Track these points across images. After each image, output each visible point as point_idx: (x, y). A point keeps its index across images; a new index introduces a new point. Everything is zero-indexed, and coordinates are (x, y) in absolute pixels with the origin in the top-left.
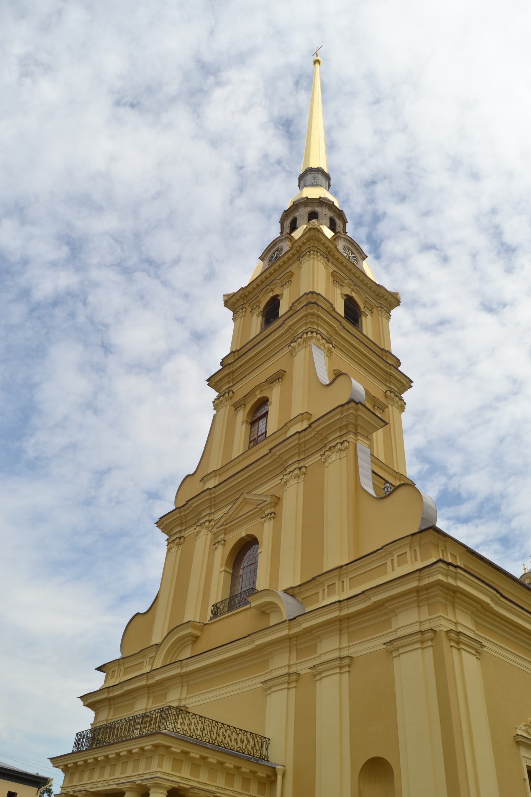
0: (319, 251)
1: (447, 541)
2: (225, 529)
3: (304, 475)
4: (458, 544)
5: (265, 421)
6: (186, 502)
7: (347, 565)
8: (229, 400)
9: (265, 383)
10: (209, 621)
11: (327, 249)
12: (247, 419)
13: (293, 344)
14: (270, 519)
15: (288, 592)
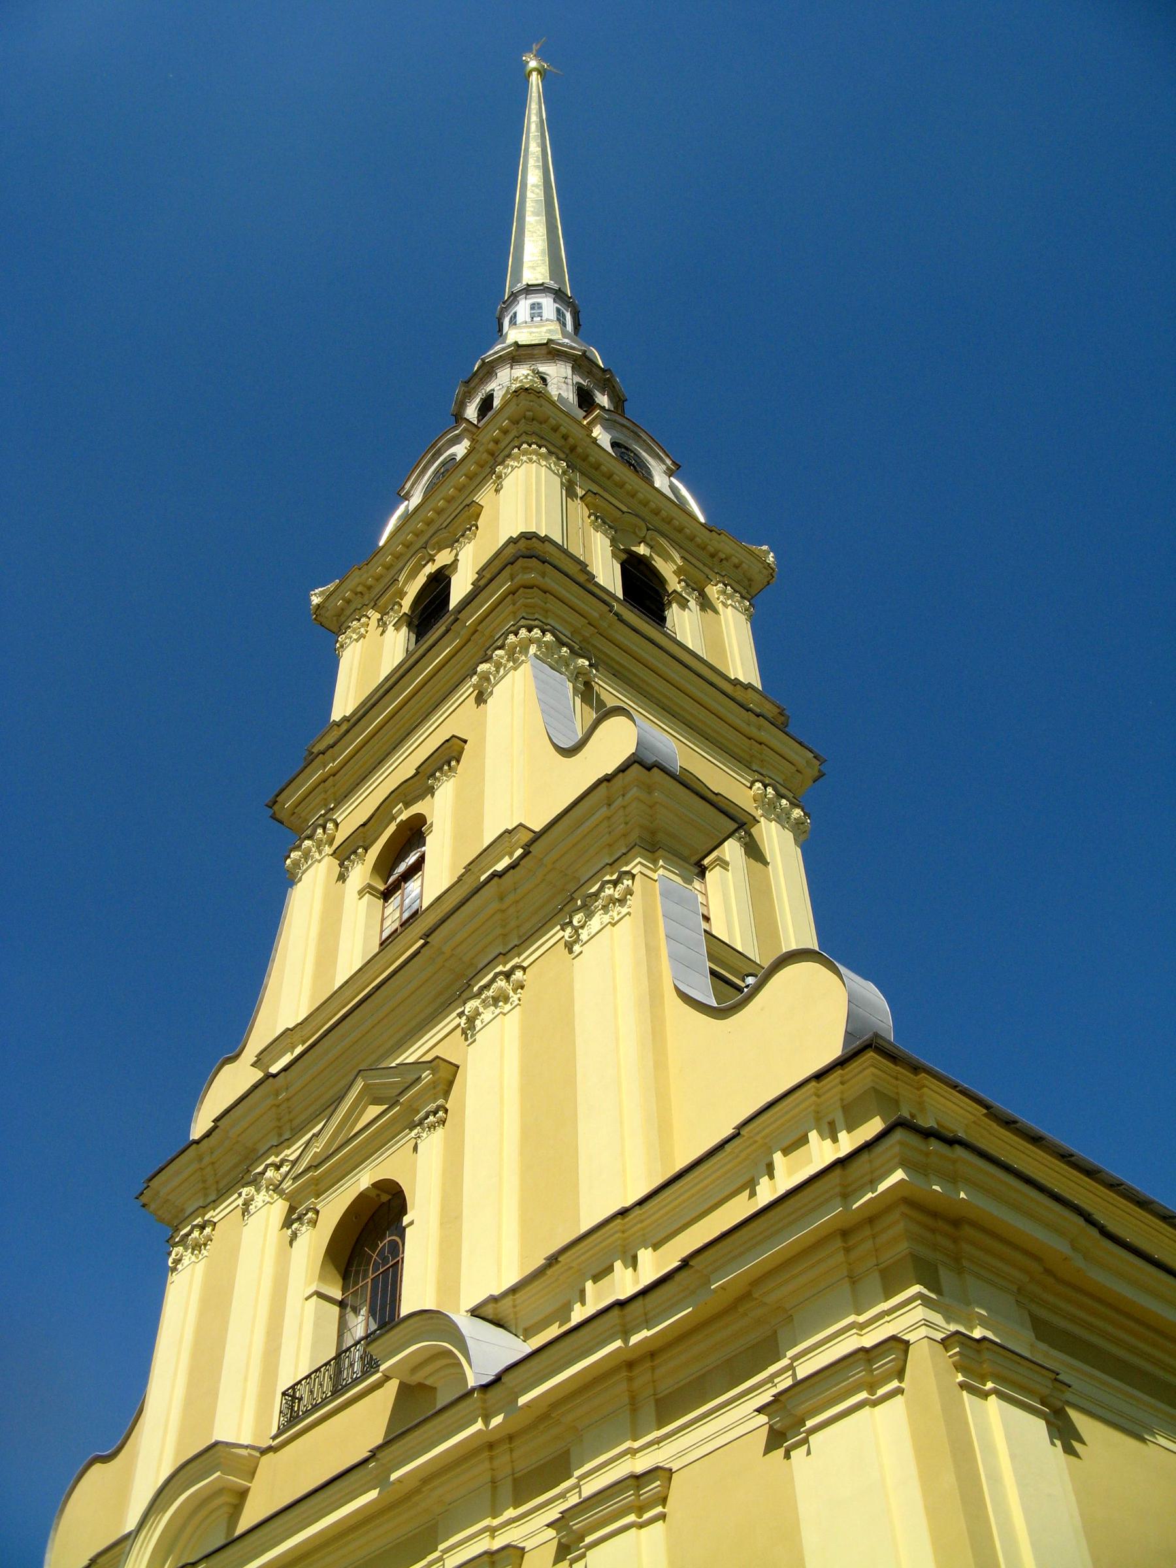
0: (543, 442)
1: (924, 1086)
2: (316, 1181)
3: (519, 991)
4: (957, 1094)
5: (419, 882)
6: (213, 1121)
7: (641, 1203)
8: (327, 846)
9: (415, 778)
10: (274, 1438)
11: (566, 440)
12: (371, 883)
13: (483, 667)
14: (432, 1127)
15: (483, 1312)
